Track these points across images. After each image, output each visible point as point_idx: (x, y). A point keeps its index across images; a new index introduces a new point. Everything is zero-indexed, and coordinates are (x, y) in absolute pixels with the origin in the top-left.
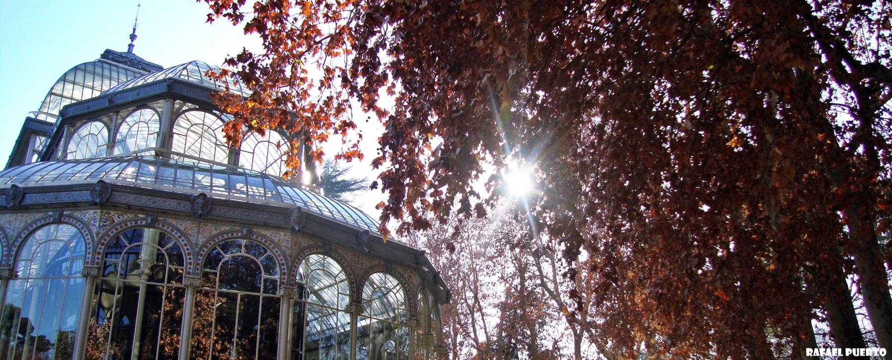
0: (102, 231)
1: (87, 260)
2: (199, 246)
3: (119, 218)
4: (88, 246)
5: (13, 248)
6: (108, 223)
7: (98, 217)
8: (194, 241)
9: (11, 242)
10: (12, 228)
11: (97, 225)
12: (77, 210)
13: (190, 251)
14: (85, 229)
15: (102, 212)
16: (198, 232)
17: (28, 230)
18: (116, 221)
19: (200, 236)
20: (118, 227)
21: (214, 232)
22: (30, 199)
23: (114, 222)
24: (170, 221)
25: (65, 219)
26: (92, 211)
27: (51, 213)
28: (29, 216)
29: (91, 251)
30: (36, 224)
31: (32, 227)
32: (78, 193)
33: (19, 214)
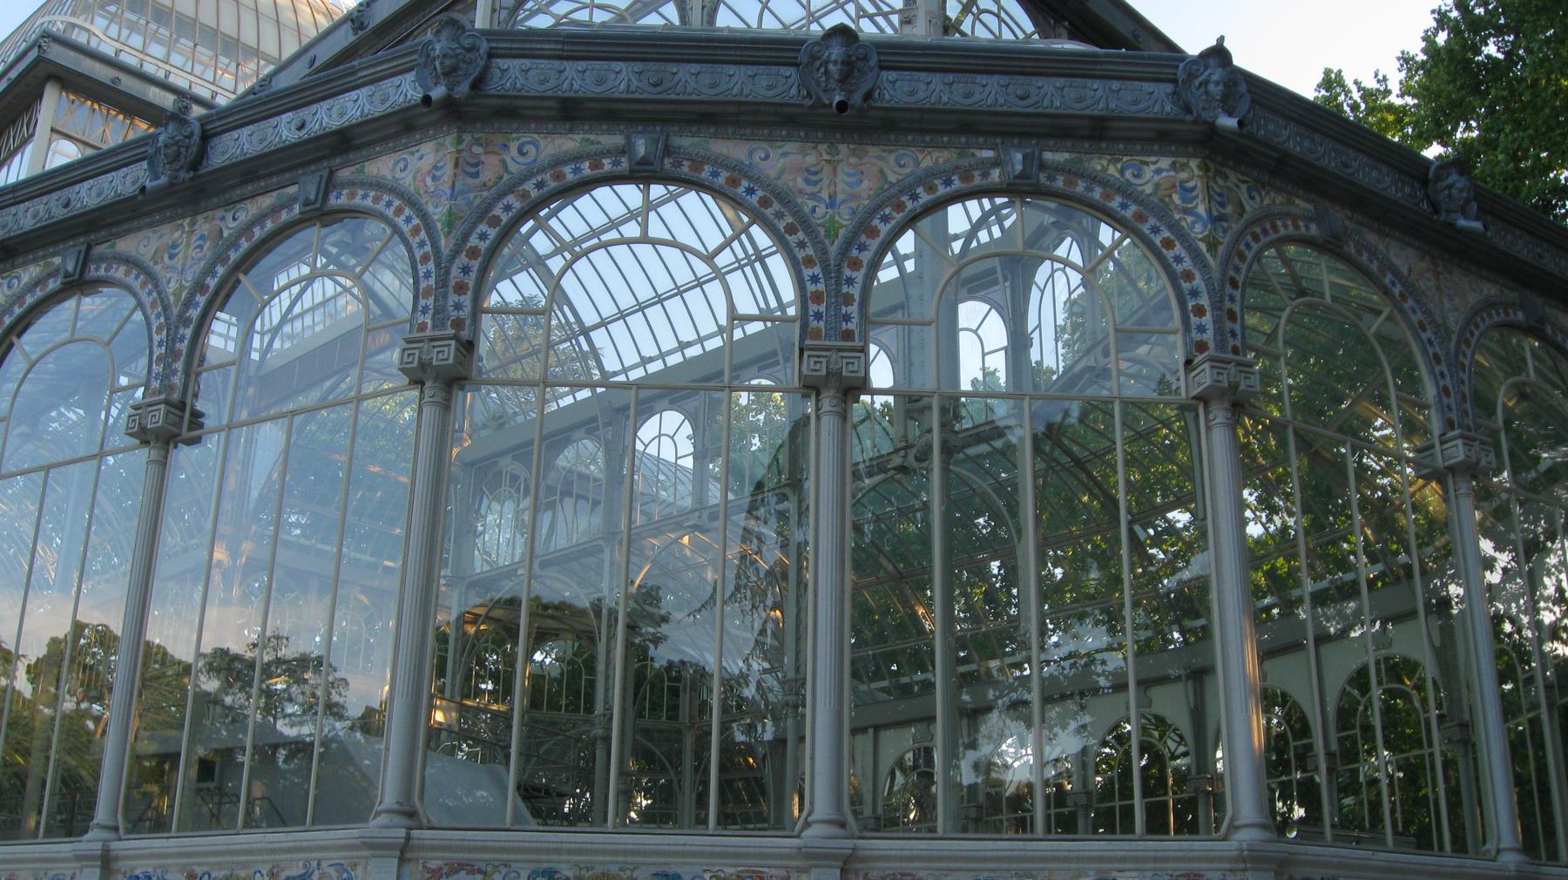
0: (1226, 240)
1: (1196, 336)
2: (1454, 337)
3: (1252, 198)
4: (1185, 286)
5: (847, 272)
6: (1229, 210)
7: (1196, 183)
8: (1438, 319)
9: (833, 249)
10: (825, 195)
11: (1201, 210)
12: (1101, 152)
13: (1438, 349)
14: (1152, 221)
15: (1204, 168)
16: (1438, 288)
17: (900, 207)
18: (1248, 208)
19: (1447, 304)
20: (1258, 230)
21: (1473, 298)
22: (899, 90)
23: (1243, 210)
24: (1372, 238)
25: (1052, 178)
26: (1165, 163)
27: (988, 154)
28: (892, 158)
29: (1204, 301)
30: (931, 189)
31: (914, 197)
32: (1115, 85)
33: (843, 148)
